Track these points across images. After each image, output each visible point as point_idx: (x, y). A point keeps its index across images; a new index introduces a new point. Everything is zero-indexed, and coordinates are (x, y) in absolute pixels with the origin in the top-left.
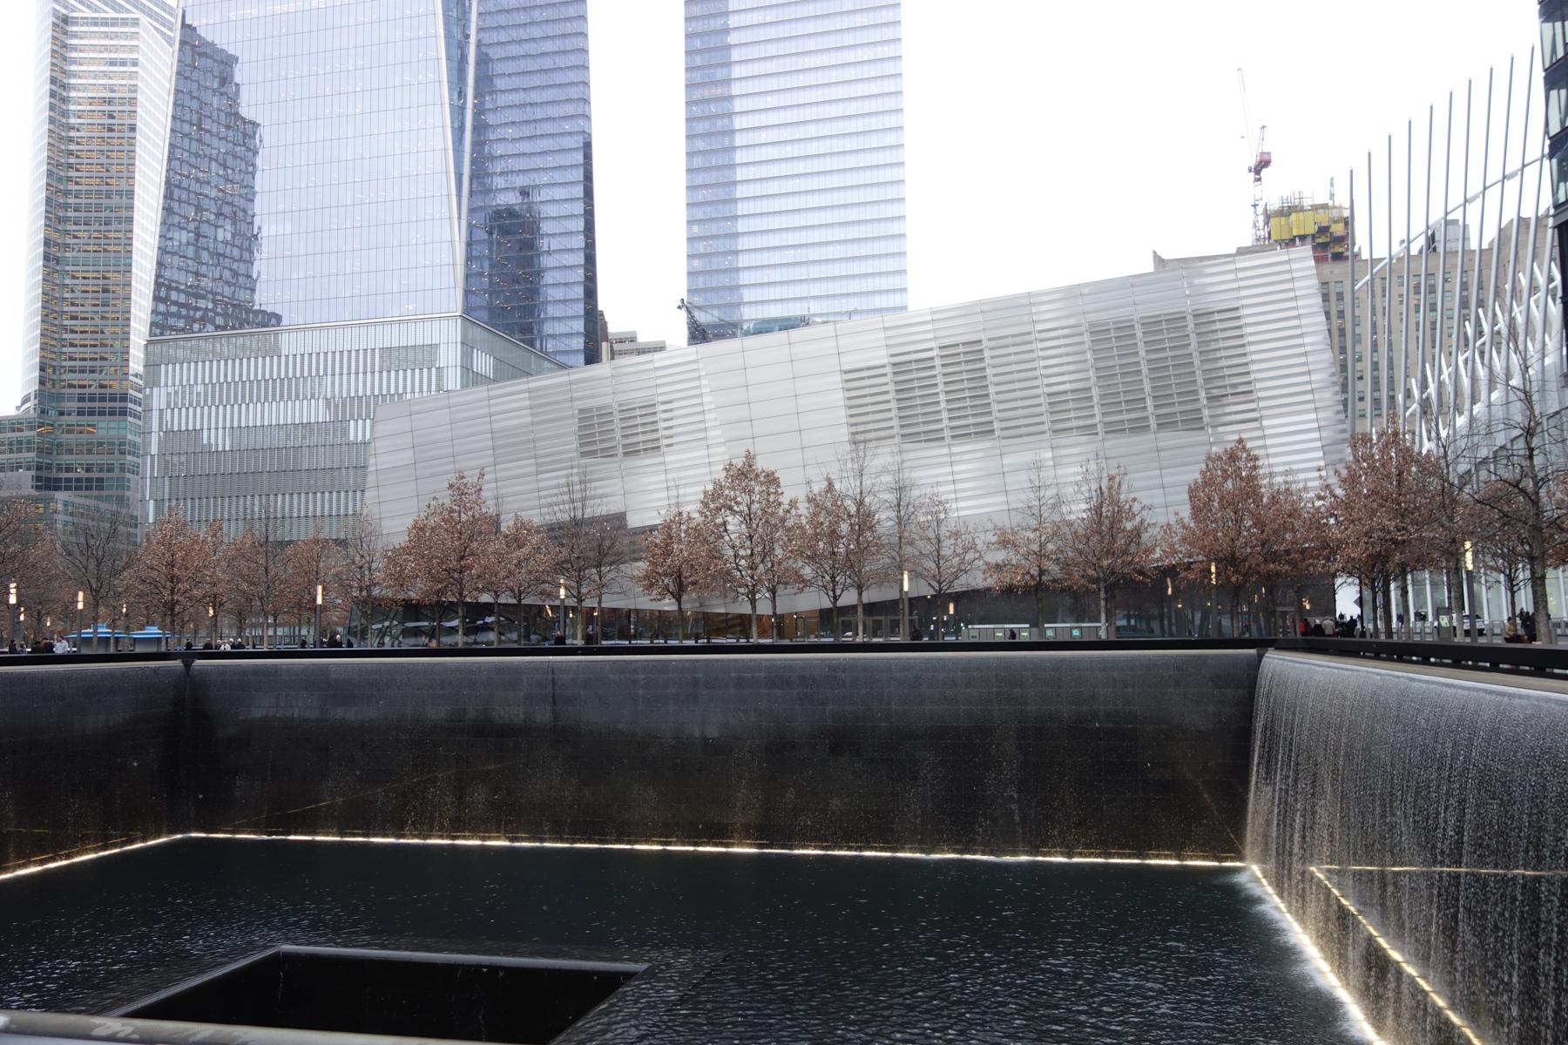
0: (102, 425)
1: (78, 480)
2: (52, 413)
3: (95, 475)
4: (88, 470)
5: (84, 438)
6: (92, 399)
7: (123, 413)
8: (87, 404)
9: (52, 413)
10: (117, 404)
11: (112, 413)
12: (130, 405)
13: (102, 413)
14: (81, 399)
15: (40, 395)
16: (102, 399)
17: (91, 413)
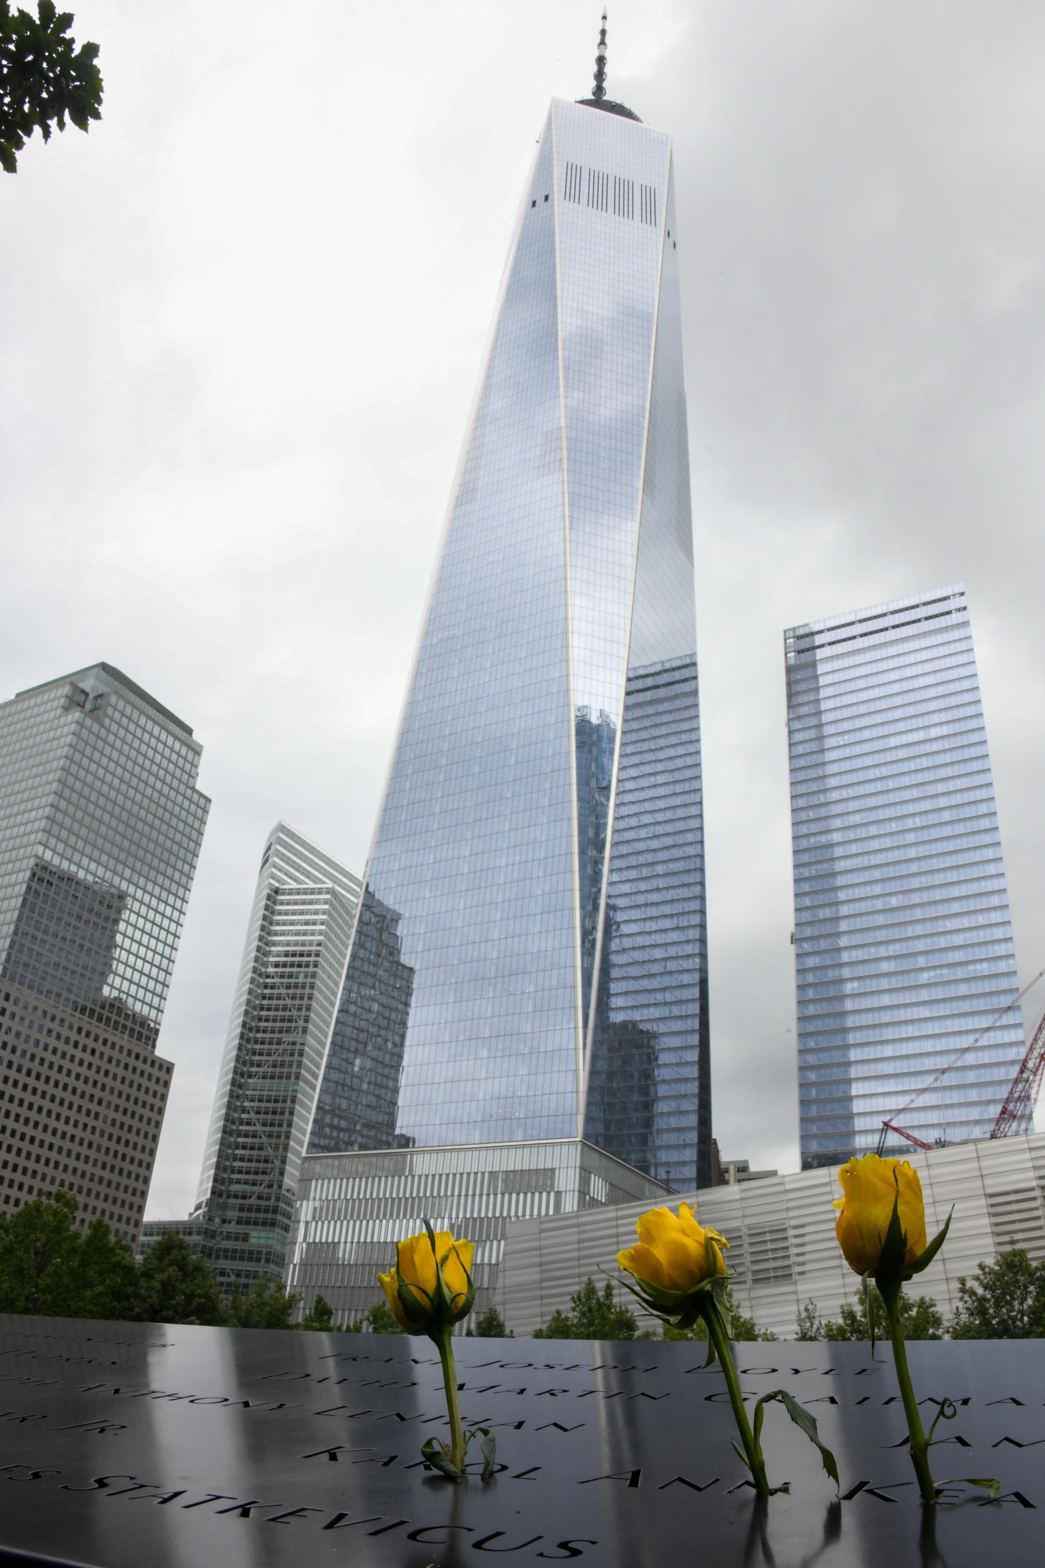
0: (254, 1234)
1: (229, 1284)
2: (217, 1220)
3: (243, 1281)
4: (238, 1275)
5: (239, 1245)
6: (250, 1210)
7: (273, 1224)
8: (245, 1214)
9: (217, 1220)
10: (270, 1216)
11: (264, 1224)
12: (279, 1217)
13: (256, 1223)
14: (242, 1209)
15: (210, 1203)
16: (258, 1211)
17: (248, 1223)
